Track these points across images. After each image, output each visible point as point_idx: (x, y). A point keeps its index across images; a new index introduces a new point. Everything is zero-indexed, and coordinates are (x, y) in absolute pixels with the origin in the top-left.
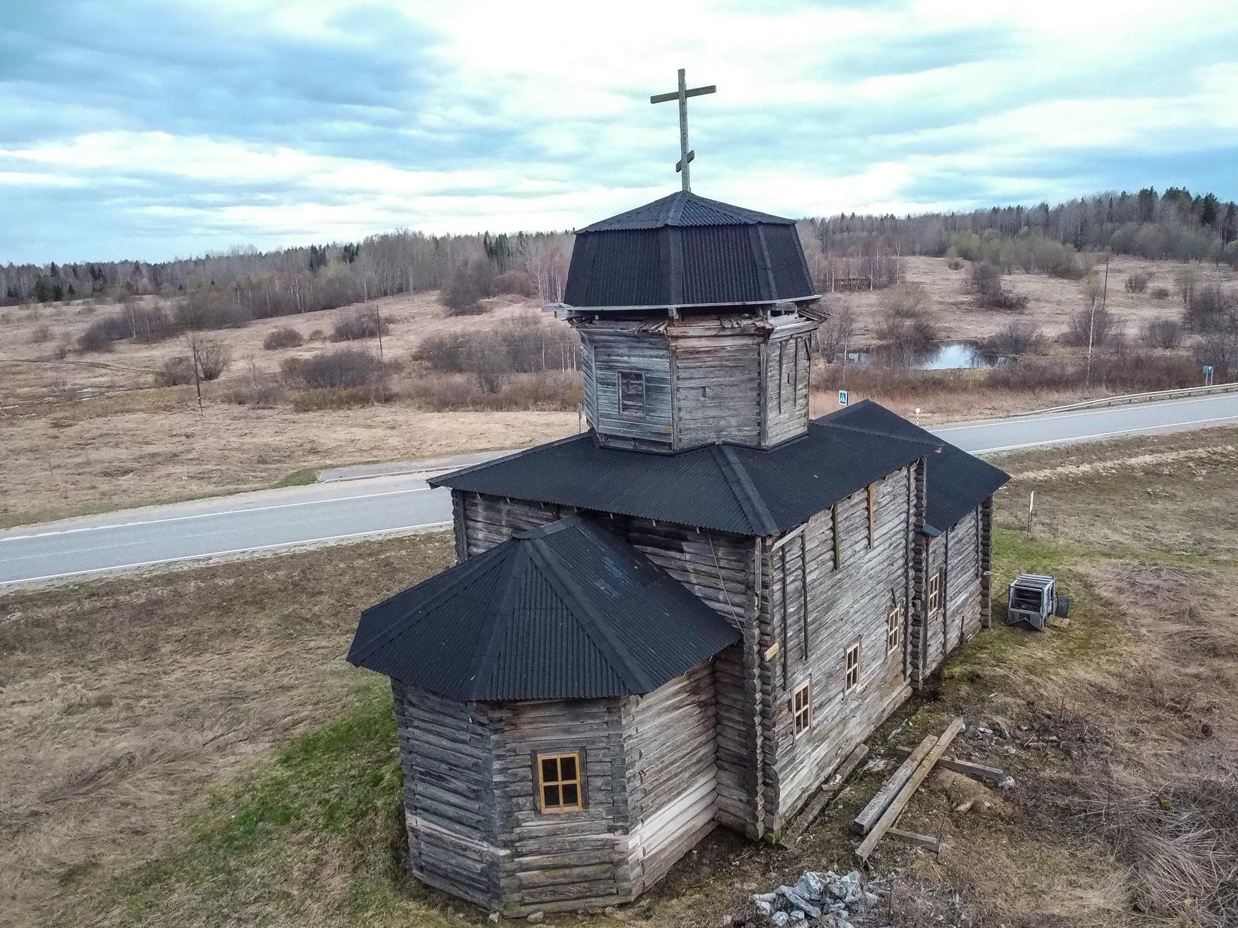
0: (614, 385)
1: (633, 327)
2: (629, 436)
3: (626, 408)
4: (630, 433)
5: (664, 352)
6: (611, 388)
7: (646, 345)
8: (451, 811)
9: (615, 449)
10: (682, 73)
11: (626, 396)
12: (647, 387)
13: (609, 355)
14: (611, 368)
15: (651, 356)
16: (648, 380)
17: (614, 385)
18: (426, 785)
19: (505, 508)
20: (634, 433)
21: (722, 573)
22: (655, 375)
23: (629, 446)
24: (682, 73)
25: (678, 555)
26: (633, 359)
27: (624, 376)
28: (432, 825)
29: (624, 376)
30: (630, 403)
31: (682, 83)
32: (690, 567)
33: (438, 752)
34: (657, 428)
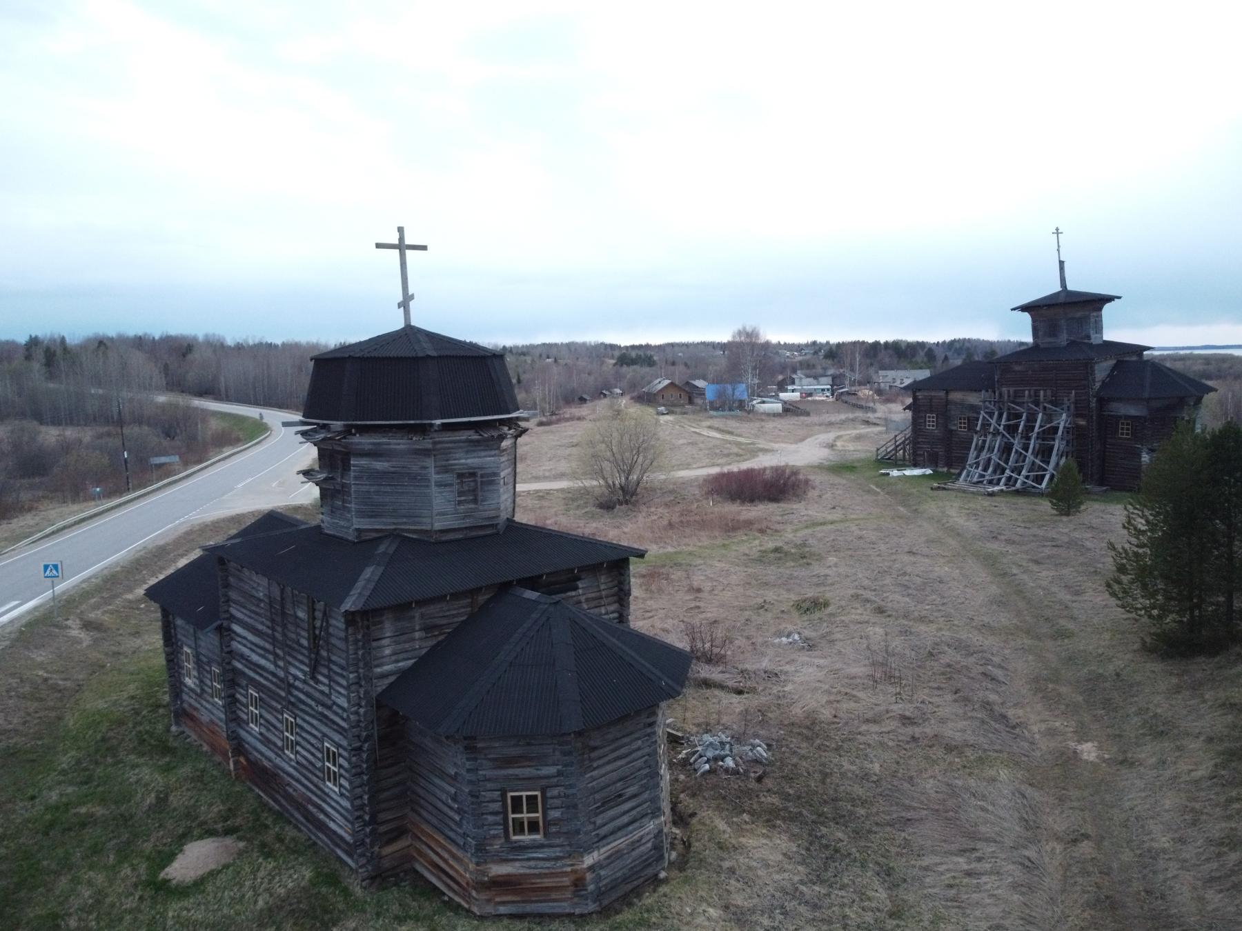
0: (451, 485)
1: (472, 435)
2: (463, 526)
3: (460, 503)
4: (463, 523)
5: (497, 452)
6: (448, 489)
7: (482, 448)
8: (625, 819)
9: (446, 542)
10: (401, 230)
11: (461, 494)
12: (481, 482)
13: (447, 460)
14: (447, 472)
15: (486, 456)
16: (482, 476)
17: (451, 485)
18: (601, 816)
19: (417, 613)
20: (468, 522)
21: (603, 593)
22: (489, 471)
23: (459, 536)
24: (401, 230)
25: (573, 593)
26: (469, 461)
27: (460, 476)
28: (609, 847)
29: (460, 476)
30: (463, 498)
31: (401, 239)
32: (583, 599)
33: (615, 775)
34: (486, 514)
